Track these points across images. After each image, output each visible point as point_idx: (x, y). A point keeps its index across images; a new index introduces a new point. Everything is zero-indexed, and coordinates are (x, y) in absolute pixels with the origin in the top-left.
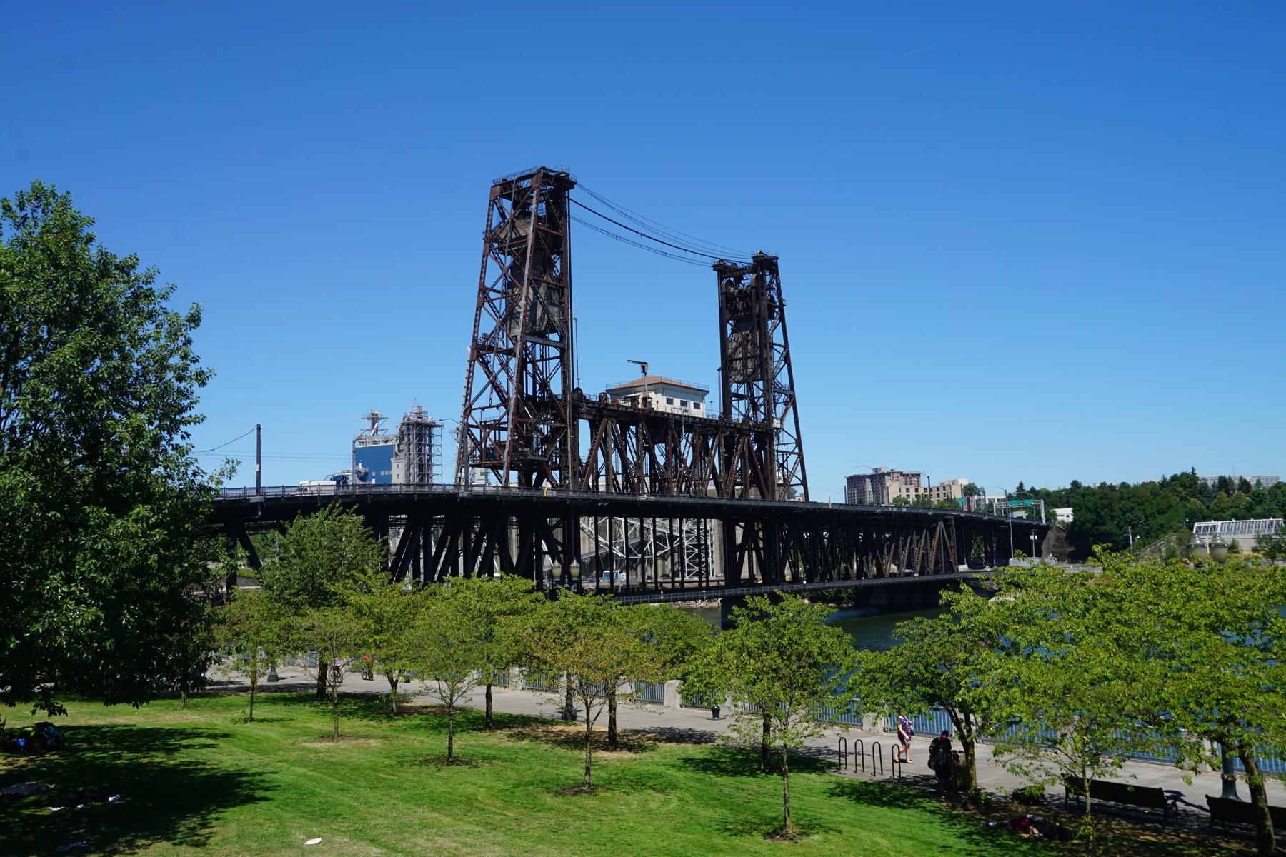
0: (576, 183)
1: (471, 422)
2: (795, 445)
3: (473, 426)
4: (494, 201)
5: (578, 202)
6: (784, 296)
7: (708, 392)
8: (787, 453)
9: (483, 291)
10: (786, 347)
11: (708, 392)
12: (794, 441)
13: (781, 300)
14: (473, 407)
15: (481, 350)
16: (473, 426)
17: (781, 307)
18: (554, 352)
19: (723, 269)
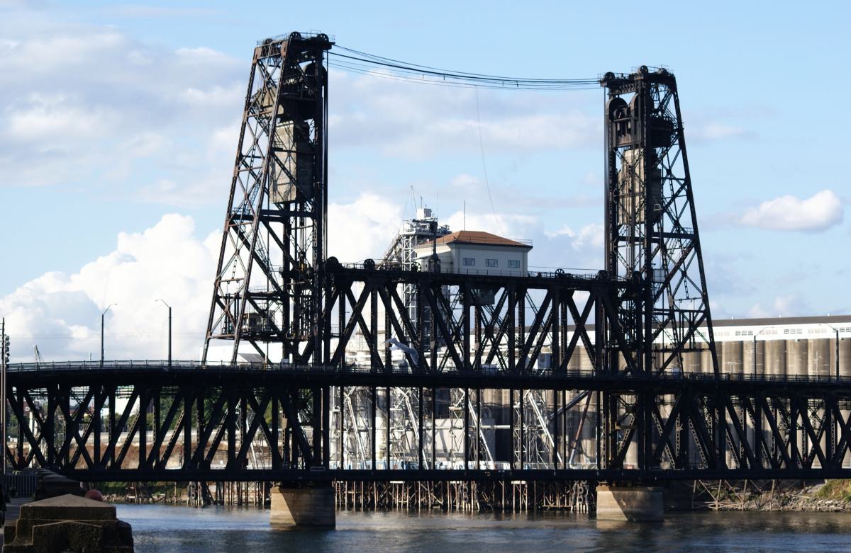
0: (333, 43)
1: (219, 294)
2: (700, 301)
3: (221, 297)
4: (258, 62)
5: (333, 64)
6: (683, 120)
7: (531, 247)
8: (694, 311)
9: (240, 158)
10: (688, 180)
11: (531, 247)
12: (700, 296)
13: (680, 123)
14: (223, 279)
15: (233, 219)
16: (221, 297)
17: (681, 130)
18: (309, 221)
19: (612, 83)
